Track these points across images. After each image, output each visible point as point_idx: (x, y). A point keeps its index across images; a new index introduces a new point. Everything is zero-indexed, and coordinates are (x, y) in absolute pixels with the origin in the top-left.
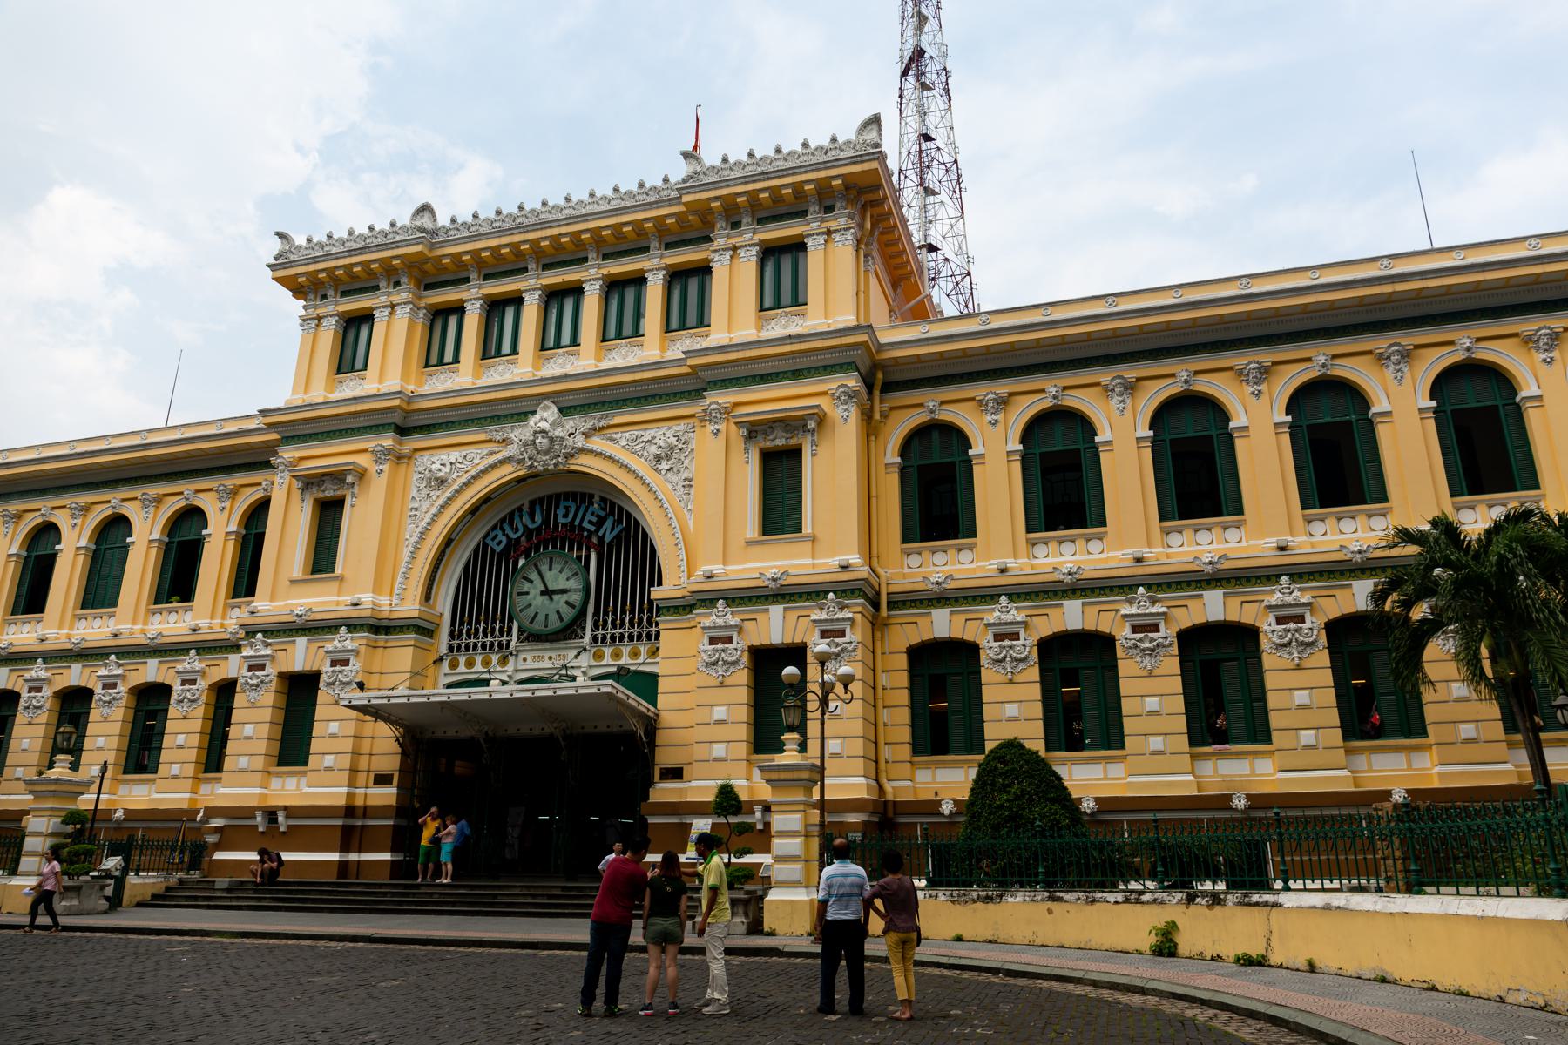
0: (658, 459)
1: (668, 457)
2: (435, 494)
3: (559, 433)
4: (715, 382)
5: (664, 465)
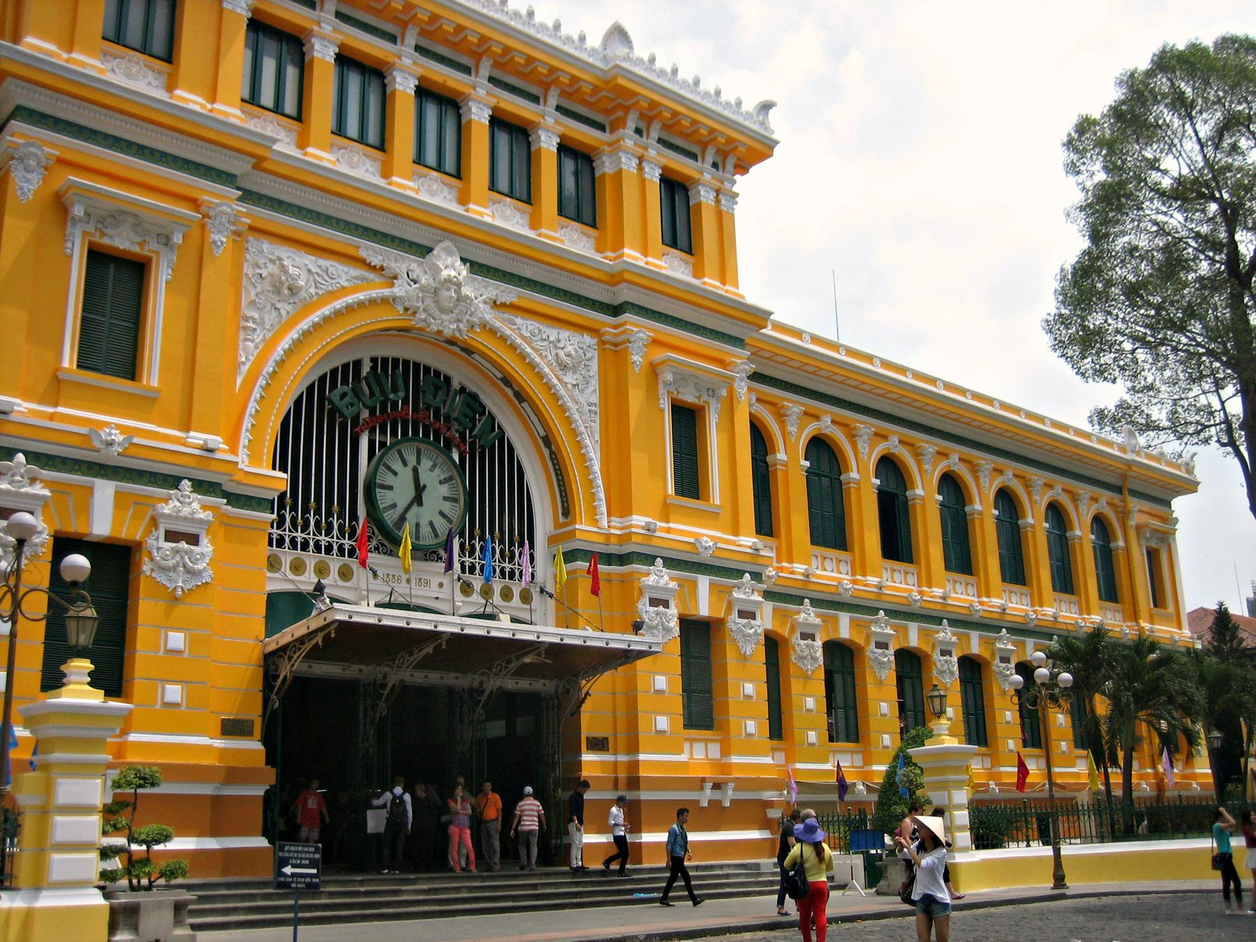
0: (564, 367)
1: (575, 369)
2: (285, 308)
3: (467, 291)
4: (633, 305)
5: (570, 379)
